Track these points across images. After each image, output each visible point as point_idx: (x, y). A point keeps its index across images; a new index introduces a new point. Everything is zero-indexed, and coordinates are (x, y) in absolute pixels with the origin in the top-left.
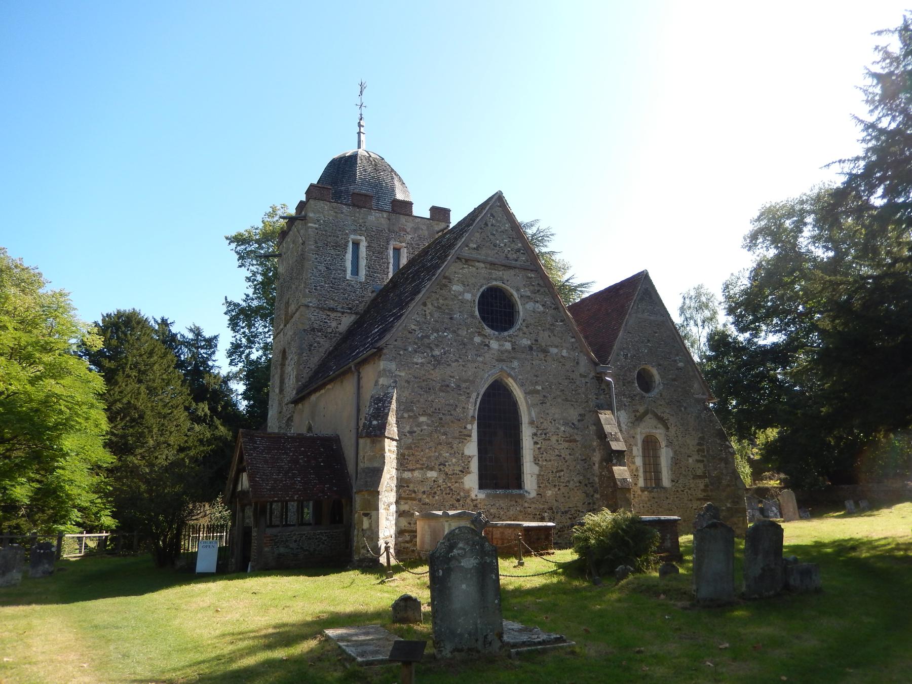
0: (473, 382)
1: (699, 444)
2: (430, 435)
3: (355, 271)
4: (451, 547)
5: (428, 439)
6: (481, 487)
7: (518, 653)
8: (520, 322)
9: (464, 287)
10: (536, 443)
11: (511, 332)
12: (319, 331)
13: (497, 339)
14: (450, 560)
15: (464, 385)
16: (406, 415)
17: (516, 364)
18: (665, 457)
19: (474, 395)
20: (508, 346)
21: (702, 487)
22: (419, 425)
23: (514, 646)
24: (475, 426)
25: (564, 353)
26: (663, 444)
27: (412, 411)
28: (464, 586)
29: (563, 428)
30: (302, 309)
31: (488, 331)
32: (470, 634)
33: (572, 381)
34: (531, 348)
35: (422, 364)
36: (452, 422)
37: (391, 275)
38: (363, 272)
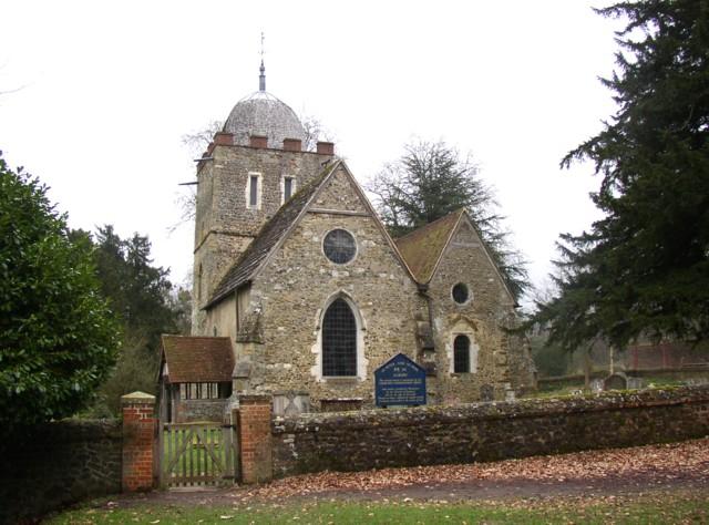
1: (503, 340)
3: (253, 202)
6: (324, 374)
8: (357, 254)
9: (312, 231)
10: (367, 343)
11: (349, 263)
12: (225, 251)
13: (338, 270)
17: (352, 287)
18: (474, 350)
19: (319, 310)
20: (347, 274)
21: (503, 372)
22: (278, 333)
24: (321, 331)
25: (392, 277)
26: (472, 340)
29: (388, 332)
30: (212, 235)
31: (331, 264)
33: (398, 298)
34: (364, 275)
37: (283, 203)
38: (259, 202)
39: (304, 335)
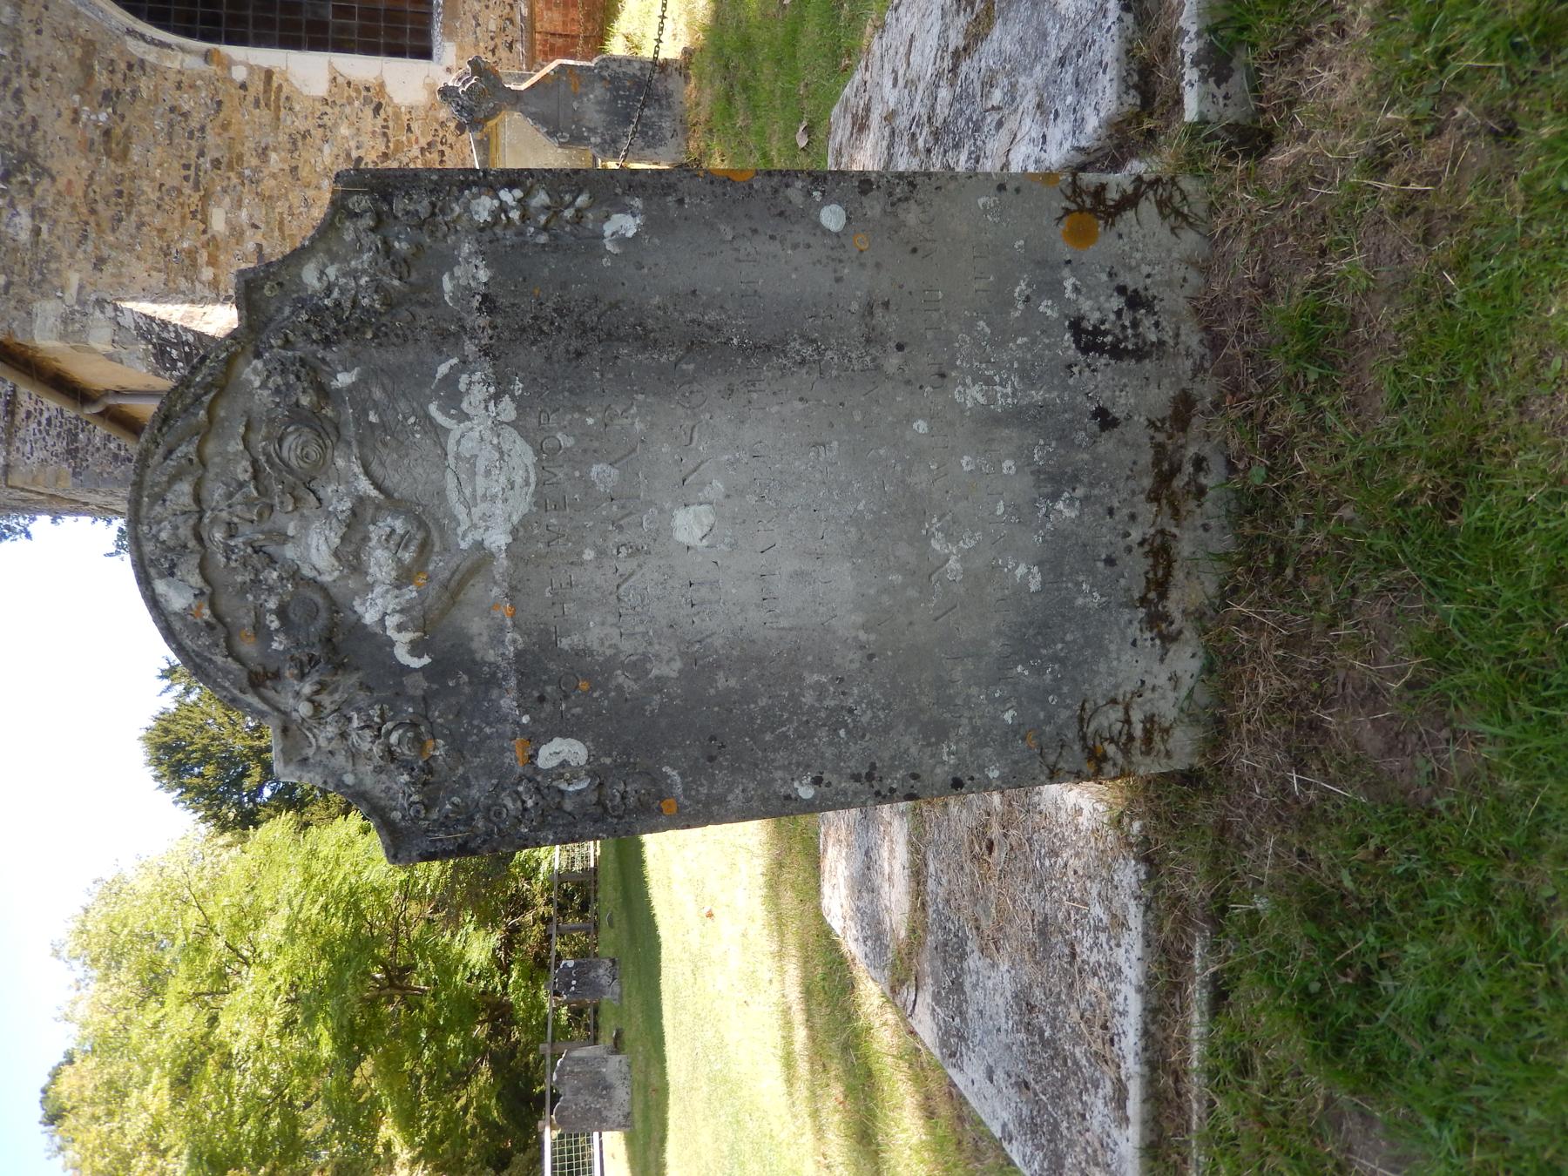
0: (89, 47)
2: (267, 200)
4: (336, 645)
5: (281, 207)
6: (425, 53)
7: (1216, 65)
12: (73, 437)
14: (450, 658)
15: (102, 79)
16: (207, 273)
19: (136, 48)
23: (1147, 82)
27: (192, 254)
28: (689, 525)
32: (1056, 481)
35: (37, 213)
36: (225, 127)
39: (249, 122)
